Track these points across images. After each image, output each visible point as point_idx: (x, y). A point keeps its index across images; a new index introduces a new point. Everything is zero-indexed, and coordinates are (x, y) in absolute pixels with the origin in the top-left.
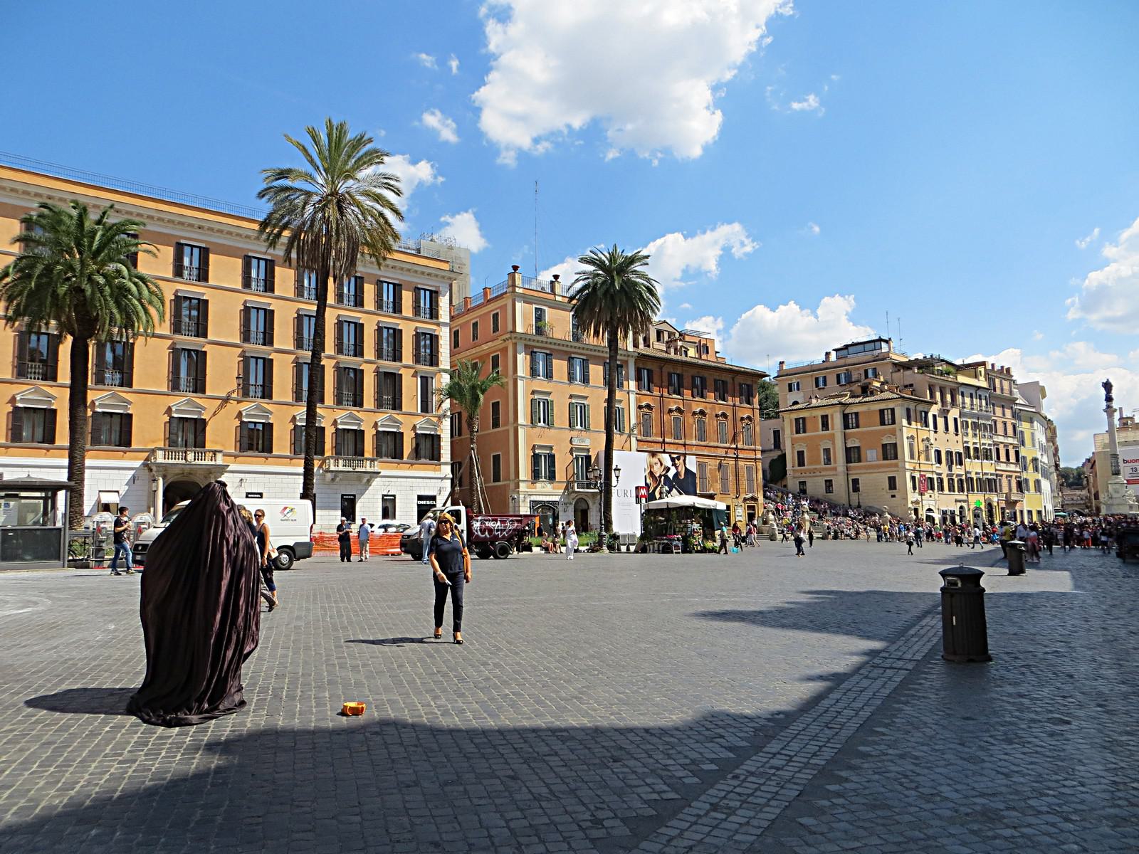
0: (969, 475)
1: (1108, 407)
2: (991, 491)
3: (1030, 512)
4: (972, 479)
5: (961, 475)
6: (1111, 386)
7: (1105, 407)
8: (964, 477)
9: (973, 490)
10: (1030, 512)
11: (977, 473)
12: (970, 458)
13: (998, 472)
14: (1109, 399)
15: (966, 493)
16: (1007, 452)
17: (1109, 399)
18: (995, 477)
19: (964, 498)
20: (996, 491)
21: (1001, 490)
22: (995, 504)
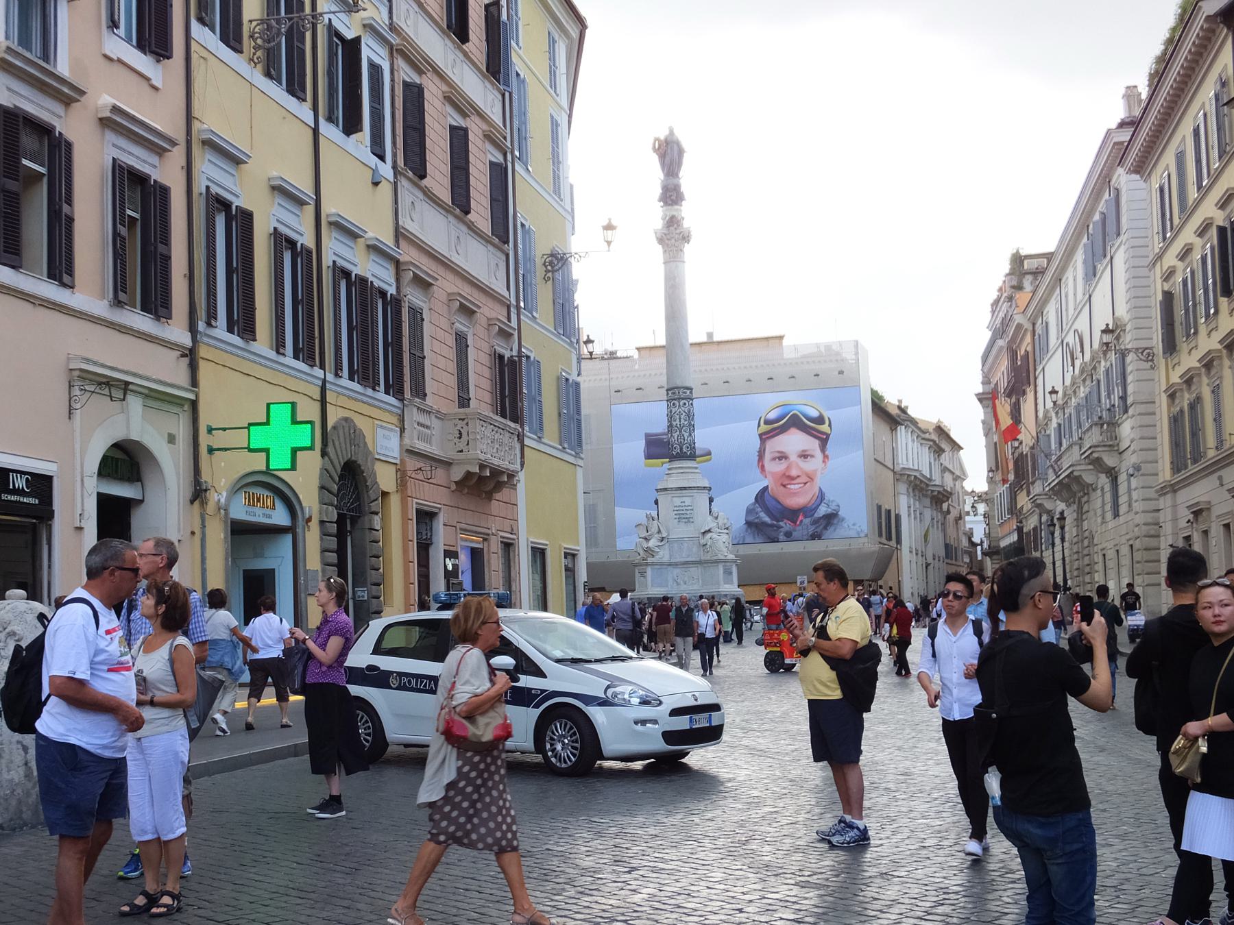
0: (210, 172)
1: (672, 222)
2: (364, 373)
3: (539, 554)
4: (242, 222)
5: (157, 145)
6: (681, 152)
7: (659, 224)
8: (167, 172)
9: (243, 325)
10: (539, 554)
11: (280, 190)
12: (231, 36)
13: (407, 254)
14: (671, 195)
15: (177, 332)
16: (459, 138)
17: (671, 195)
18: (380, 275)
19: (171, 371)
20: (394, 388)
21: (419, 391)
22: (385, 479)
